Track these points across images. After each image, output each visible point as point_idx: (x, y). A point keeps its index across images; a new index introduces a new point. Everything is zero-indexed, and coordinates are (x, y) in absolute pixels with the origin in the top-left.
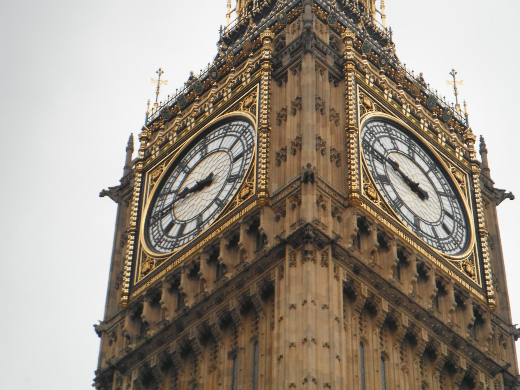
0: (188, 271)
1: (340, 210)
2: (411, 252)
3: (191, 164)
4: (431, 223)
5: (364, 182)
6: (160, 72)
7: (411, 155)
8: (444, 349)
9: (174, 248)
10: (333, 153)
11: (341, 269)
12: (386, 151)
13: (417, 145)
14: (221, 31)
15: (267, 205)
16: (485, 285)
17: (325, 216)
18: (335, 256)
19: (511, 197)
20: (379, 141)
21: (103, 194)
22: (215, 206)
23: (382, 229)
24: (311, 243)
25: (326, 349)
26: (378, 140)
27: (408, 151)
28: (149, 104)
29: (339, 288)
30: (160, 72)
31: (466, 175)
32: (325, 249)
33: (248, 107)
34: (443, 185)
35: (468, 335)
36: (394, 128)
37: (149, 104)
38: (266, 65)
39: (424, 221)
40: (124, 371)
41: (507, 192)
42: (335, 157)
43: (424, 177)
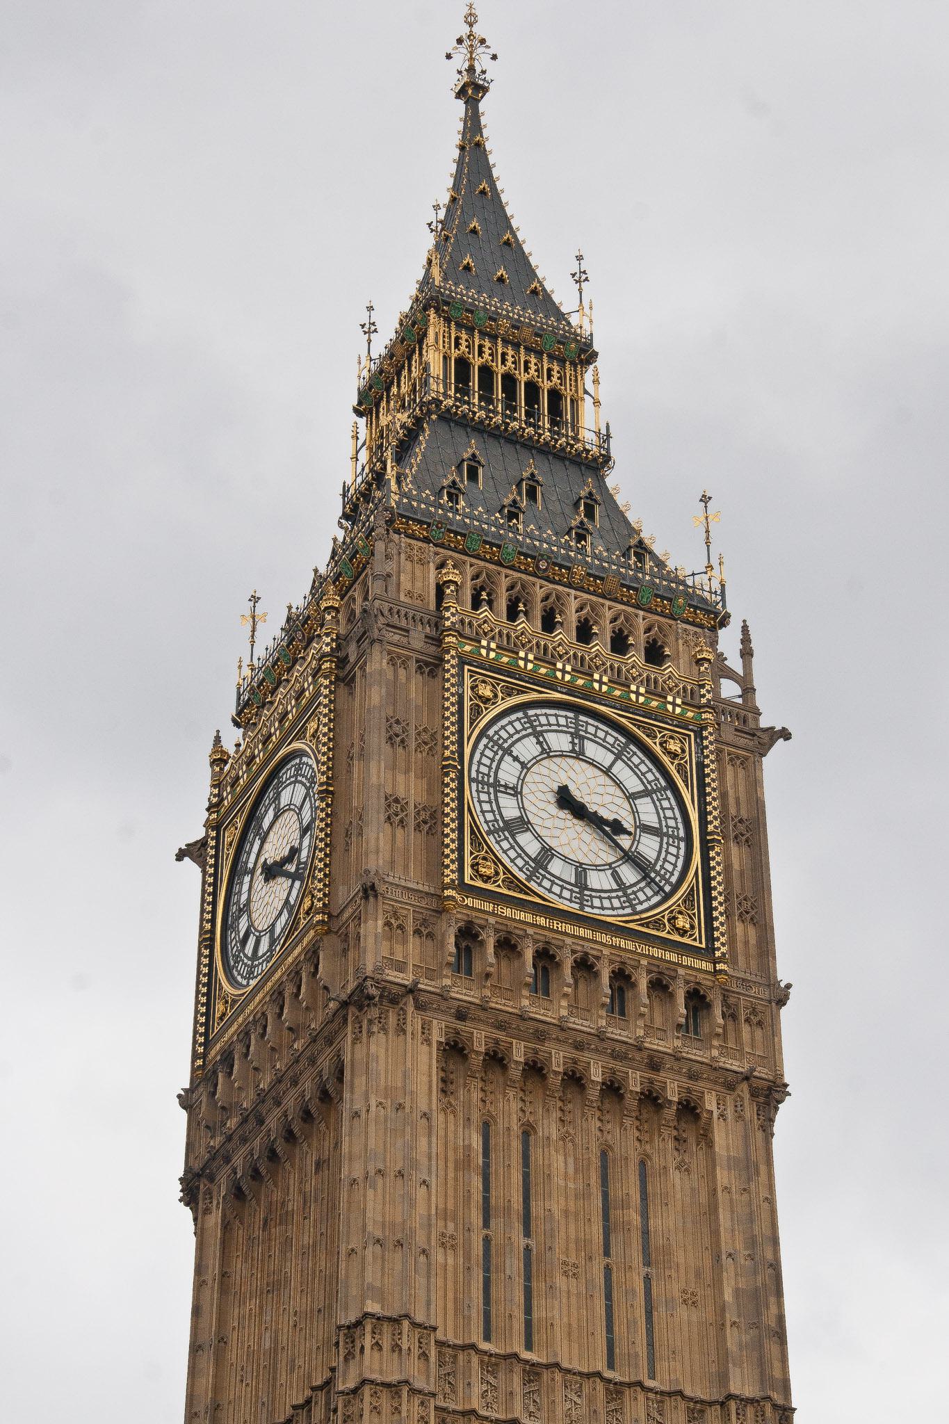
0: (260, 1030)
1: (432, 920)
2: (560, 943)
3: (266, 824)
4: (610, 865)
5: (472, 853)
6: (255, 599)
7: (577, 748)
8: (635, 1082)
9: (249, 979)
10: (423, 816)
11: (435, 1022)
12: (523, 765)
13: (590, 721)
14: (344, 496)
15: (328, 932)
16: (711, 939)
17: (405, 942)
18: (419, 1007)
19: (785, 734)
20: (510, 754)
21: (180, 856)
22: (285, 915)
23: (504, 928)
24: (375, 1005)
25: (399, 1180)
26: (508, 752)
27: (572, 742)
28: (240, 667)
29: (431, 1059)
30: (255, 599)
31: (689, 736)
32: (401, 1005)
33: (313, 736)
34: (640, 777)
35: (678, 1043)
36: (544, 711)
37: (240, 667)
38: (327, 665)
39: (597, 867)
40: (211, 1179)
41: (778, 728)
42: (425, 822)
43: (603, 779)
